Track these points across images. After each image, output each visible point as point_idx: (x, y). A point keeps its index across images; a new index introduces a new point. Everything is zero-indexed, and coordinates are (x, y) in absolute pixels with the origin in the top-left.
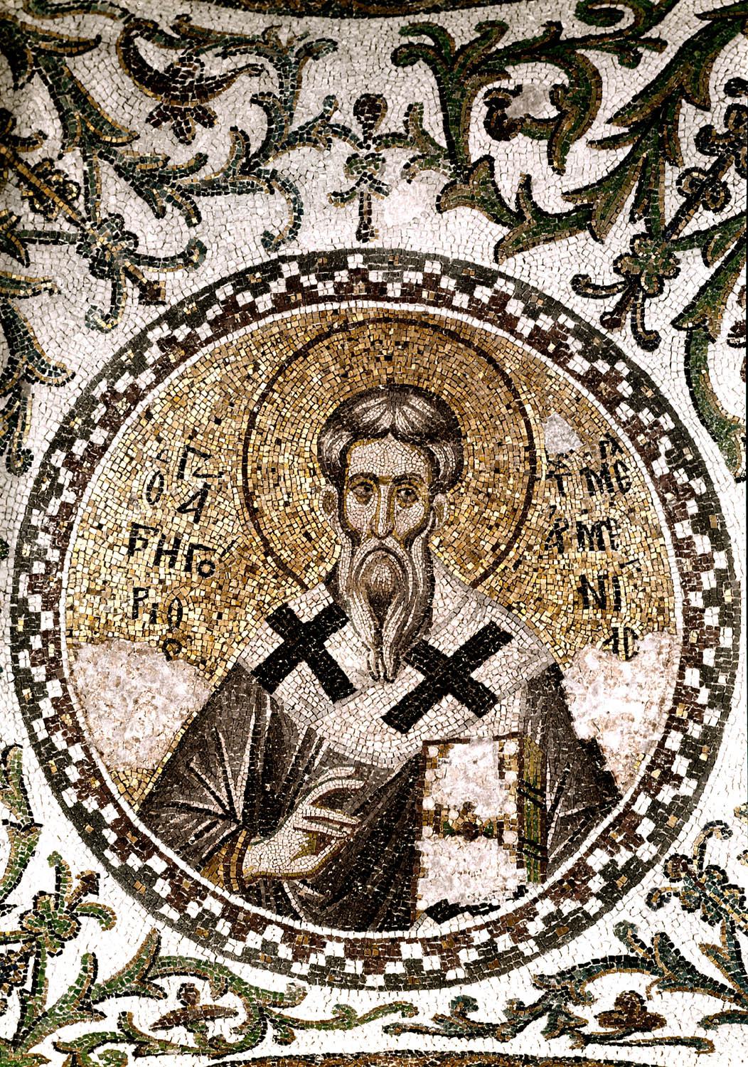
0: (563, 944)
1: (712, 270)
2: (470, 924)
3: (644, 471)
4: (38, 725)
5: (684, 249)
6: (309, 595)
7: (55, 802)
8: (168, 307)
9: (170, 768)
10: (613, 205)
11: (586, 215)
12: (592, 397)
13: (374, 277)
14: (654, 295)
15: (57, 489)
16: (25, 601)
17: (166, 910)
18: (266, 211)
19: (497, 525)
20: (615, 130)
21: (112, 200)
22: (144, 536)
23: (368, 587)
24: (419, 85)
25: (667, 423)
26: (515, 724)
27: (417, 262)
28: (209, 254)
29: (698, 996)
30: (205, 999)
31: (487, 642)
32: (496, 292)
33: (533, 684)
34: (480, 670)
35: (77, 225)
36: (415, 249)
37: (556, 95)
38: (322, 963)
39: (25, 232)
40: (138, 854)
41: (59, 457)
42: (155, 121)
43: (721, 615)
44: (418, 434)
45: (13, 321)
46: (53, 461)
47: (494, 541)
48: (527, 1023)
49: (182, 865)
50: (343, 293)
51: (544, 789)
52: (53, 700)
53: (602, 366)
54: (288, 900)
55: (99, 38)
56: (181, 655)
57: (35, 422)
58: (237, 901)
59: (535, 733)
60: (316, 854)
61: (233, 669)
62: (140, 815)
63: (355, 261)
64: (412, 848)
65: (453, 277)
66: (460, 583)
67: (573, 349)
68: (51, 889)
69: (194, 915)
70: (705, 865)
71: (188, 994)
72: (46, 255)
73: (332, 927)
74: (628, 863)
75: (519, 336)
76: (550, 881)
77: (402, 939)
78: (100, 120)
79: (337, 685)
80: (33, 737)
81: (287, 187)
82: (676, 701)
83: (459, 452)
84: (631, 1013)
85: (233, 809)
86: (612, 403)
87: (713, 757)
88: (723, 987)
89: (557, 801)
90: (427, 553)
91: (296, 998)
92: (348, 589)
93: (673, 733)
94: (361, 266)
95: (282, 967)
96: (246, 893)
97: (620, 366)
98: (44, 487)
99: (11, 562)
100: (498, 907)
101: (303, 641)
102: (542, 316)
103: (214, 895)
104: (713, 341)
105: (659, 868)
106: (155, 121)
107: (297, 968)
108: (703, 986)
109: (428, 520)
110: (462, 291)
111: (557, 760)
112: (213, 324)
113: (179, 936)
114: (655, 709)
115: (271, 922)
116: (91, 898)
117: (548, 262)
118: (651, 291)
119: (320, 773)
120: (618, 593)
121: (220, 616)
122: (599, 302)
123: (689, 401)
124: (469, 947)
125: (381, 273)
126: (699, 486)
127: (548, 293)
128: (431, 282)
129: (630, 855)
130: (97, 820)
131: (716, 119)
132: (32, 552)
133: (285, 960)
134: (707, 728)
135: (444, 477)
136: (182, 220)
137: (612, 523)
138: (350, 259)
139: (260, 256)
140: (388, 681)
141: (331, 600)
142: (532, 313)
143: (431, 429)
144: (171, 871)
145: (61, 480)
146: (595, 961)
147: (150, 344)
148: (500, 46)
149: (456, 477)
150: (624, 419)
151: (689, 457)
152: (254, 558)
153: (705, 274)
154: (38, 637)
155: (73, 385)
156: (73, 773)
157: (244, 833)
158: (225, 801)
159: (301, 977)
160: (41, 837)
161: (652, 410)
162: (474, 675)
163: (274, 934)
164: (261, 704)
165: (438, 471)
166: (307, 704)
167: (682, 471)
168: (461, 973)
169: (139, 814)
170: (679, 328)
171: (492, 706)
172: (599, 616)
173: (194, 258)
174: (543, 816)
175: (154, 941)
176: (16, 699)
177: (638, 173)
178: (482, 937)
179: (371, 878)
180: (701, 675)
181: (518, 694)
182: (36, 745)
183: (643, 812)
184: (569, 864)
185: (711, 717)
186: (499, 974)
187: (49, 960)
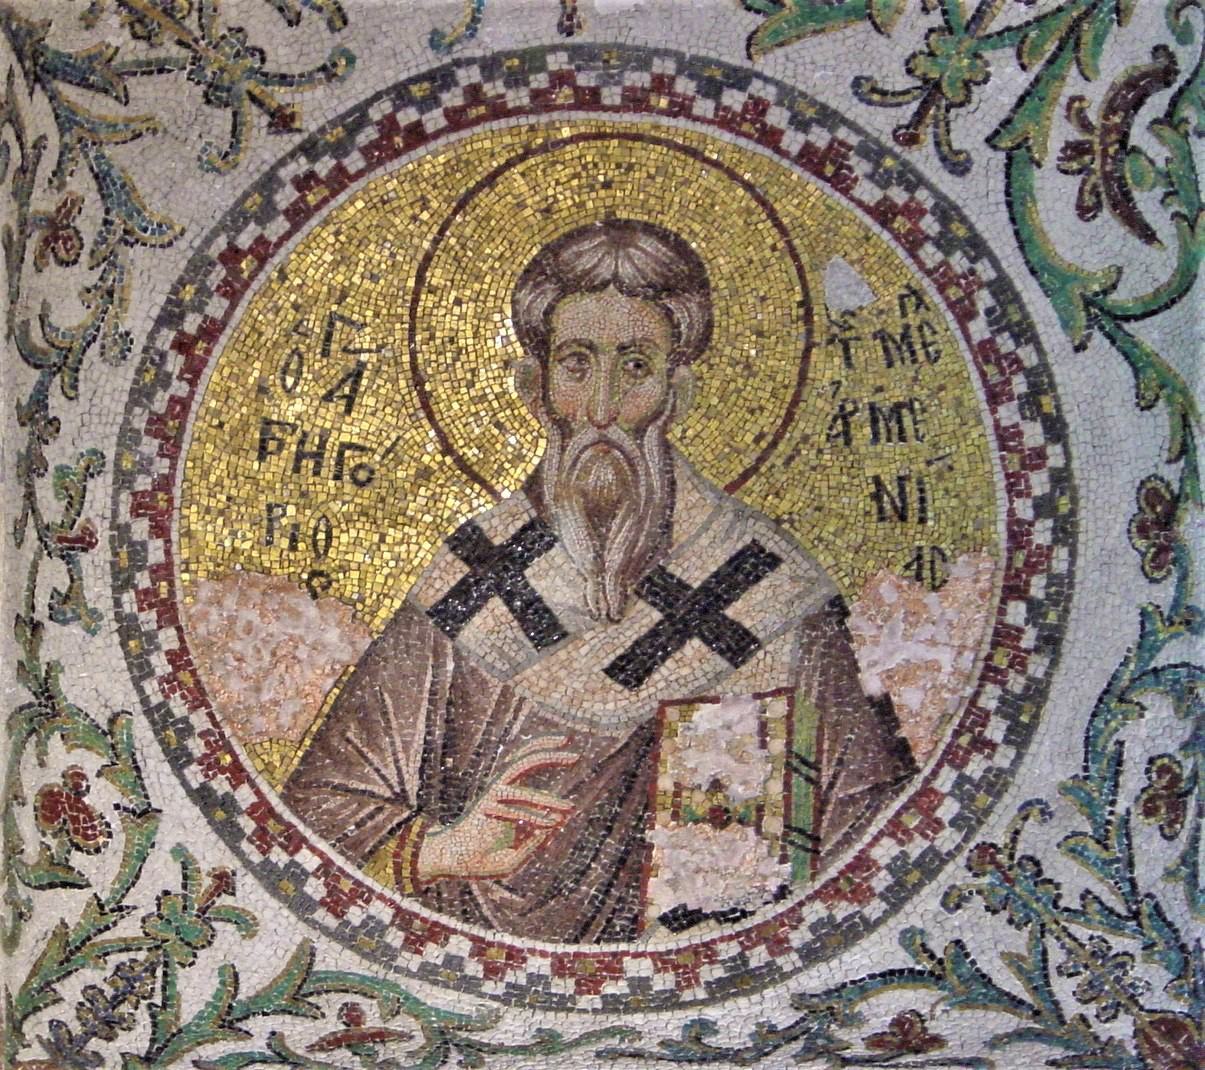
0: (834, 956)
1: (1032, 77)
2: (716, 935)
3: (958, 334)
4: (151, 687)
5: (994, 48)
6: (504, 508)
7: (175, 781)
8: (306, 135)
9: (320, 739)
12: (886, 236)
13: (584, 80)
14: (961, 105)
15: (164, 381)
16: (128, 526)
17: (321, 915)
19: (762, 409)
22: (279, 435)
23: (584, 494)
26: (783, 677)
27: (642, 58)
28: (359, 63)
29: (992, 1015)
30: (372, 1020)
31: (749, 566)
32: (751, 97)
33: (811, 623)
34: (738, 604)
35: (188, 46)
36: (638, 42)
38: (523, 981)
39: (123, 64)
40: (284, 848)
41: (167, 336)
43: (1054, 530)
44: (650, 285)
45: (108, 174)
46: (158, 344)
47: (756, 430)
48: (776, 1047)
49: (339, 861)
50: (541, 101)
51: (819, 761)
52: (167, 653)
53: (898, 195)
54: (477, 905)
56: (331, 591)
57: (134, 295)
58: (411, 905)
59: (809, 686)
60: (515, 847)
61: (402, 609)
62: (286, 798)
63: (557, 62)
64: (643, 840)
65: (691, 77)
66: (713, 488)
69: (356, 922)
70: (1018, 855)
71: (352, 1015)
72: (150, 88)
73: (536, 938)
74: (923, 855)
75: (785, 154)
76: (823, 878)
77: (626, 953)
79: (541, 624)
80: (145, 701)
82: (995, 645)
83: (707, 307)
84: (906, 1034)
85: (403, 791)
86: (913, 243)
87: (1036, 717)
88: (1021, 1002)
89: (835, 776)
90: (666, 447)
91: (490, 1021)
92: (556, 498)
93: (989, 687)
94: (565, 67)
95: (469, 985)
96: (422, 893)
97: (922, 195)
98: (148, 378)
99: (110, 478)
100: (753, 913)
102: (815, 129)
103: (381, 897)
104: (1039, 165)
105: (961, 860)
107: (489, 987)
108: (998, 1001)
109: (665, 402)
110: (706, 95)
111: (837, 723)
112: (366, 151)
113: (338, 947)
114: (969, 655)
115: (454, 931)
116: (225, 900)
117: (819, 59)
118: (958, 100)
119: (516, 743)
120: (922, 500)
121: (382, 539)
122: (892, 111)
123: (1014, 243)
124: (712, 962)
125: (593, 74)
126: (1028, 356)
127: (821, 99)
128: (661, 84)
129: (926, 844)
130: (228, 803)
132: (134, 463)
133: (474, 978)
134: (1031, 679)
135: (688, 344)
136: (323, 25)
137: (917, 405)
138: (550, 58)
139: (430, 61)
140: (612, 621)
141: (534, 514)
142: (801, 124)
143: (667, 279)
145: (169, 367)
146: (872, 977)
147: (282, 184)
149: (704, 342)
150: (930, 265)
151: (1016, 318)
152: (426, 459)
153: (1023, 80)
154: (146, 573)
155: (182, 244)
156: (197, 747)
157: (418, 822)
158: (394, 781)
159: (494, 998)
160: (161, 825)
161: (965, 253)
162: (729, 612)
163: (459, 946)
164: (438, 653)
165: (679, 336)
166: (502, 654)
167: (1006, 335)
168: (702, 994)
169: (282, 796)
170: (995, 148)
171: (752, 653)
172: (898, 531)
173: (340, 71)
174: (817, 795)
175: (307, 953)
176: (121, 654)
179: (591, 881)
180: (1029, 610)
181: (790, 637)
182: (148, 712)
183: (946, 789)
184: (848, 856)
185: (1037, 666)
186: (746, 993)
187: (180, 971)
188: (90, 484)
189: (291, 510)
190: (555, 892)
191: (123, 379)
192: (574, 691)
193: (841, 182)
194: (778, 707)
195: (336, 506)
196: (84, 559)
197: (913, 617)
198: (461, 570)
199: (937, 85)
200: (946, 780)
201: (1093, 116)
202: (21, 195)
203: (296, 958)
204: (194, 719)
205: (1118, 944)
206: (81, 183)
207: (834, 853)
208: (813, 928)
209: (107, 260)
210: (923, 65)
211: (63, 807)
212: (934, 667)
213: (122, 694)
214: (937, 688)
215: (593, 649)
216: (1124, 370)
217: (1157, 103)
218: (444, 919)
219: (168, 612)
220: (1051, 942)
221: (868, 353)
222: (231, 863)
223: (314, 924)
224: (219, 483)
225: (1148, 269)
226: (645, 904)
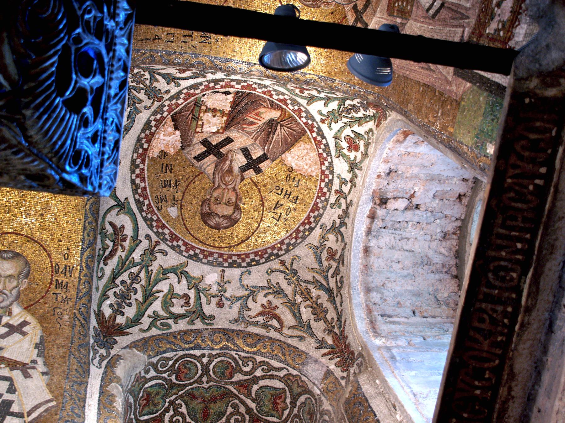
4: (329, 160)
9: (296, 141)
10: (158, 274)
11: (165, 272)
12: (164, 222)
13: (221, 260)
15: (314, 217)
17: (304, 110)
18: (250, 281)
20: (157, 295)
21: (289, 289)
24: (208, 310)
25: (144, 214)
27: (209, 263)
31: (199, 158)
33: (189, 146)
37: (173, 305)
41: (313, 225)
49: (297, 118)
50: (230, 256)
53: (160, 230)
55: (289, 329)
57: (318, 236)
63: (226, 264)
67: (168, 235)
68: (333, 123)
71: (302, 92)
75: (182, 240)
76: (195, 97)
78: (290, 309)
79: (246, 152)
80: (331, 158)
81: (243, 286)
83: (202, 210)
86: (158, 220)
90: (214, 182)
92: (238, 176)
95: (275, 90)
96: (282, 109)
97: (155, 230)
101: (253, 164)
105: (165, 99)
107: (271, 89)
112: (266, 253)
114: (157, 137)
116: (323, 118)
119: (255, 131)
126: (137, 197)
128: (205, 257)
131: (133, 297)
134: (144, 133)
139: (252, 269)
142: (179, 246)
144: (300, 117)
148: (188, 318)
149: (203, 202)
150: (155, 216)
153: (133, 255)
155: (306, 243)
156: (322, 146)
158: (282, 129)
162: (206, 149)
163: (275, 97)
164: (268, 150)
166: (255, 148)
177: (151, 283)
181: (194, 143)
188: (334, 202)
189: (294, 185)
190: (253, 102)
191: (323, 220)
192: (240, 139)
193: (171, 233)
194: (198, 130)
195: (284, 184)
196: (338, 188)
197: (167, 145)
198: (261, 165)
199: (151, 254)
200: (165, 114)
201: (120, 247)
202: (337, 269)
203: (311, 104)
204: (322, 152)
205: (134, 84)
206: (325, 263)
207: (191, 102)
208: (199, 88)
210: (153, 258)
211: (353, 147)
212: (164, 135)
214: (164, 131)
215: (236, 145)
217: (107, 253)
218: (278, 102)
219: (323, 172)
220: (148, 84)
221: (169, 198)
222: (320, 124)
223: (306, 108)
224: (307, 194)
225: (111, 217)
226: (234, 97)
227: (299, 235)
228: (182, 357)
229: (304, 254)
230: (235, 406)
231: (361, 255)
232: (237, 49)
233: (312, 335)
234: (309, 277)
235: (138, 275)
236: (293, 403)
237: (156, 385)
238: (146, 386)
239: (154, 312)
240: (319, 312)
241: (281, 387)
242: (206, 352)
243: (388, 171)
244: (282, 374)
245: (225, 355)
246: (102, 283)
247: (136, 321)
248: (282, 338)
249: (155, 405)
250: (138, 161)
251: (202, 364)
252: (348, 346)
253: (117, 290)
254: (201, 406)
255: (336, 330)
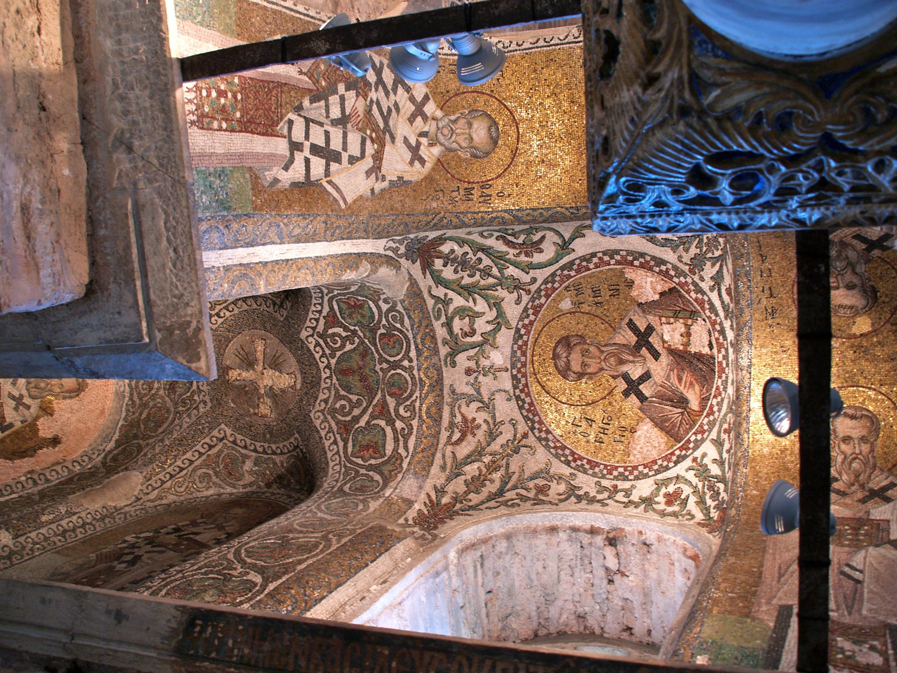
4: (651, 474)
10: (494, 297)
11: (496, 305)
13: (519, 365)
17: (705, 436)
18: (499, 399)
20: (471, 300)
24: (461, 358)
25: (559, 272)
27: (514, 353)
31: (632, 325)
33: (644, 312)
41: (573, 464)
42: (474, 435)
50: (524, 375)
53: (543, 293)
71: (725, 431)
79: (646, 377)
81: (493, 394)
83: (573, 336)
90: (606, 345)
95: (722, 400)
96: (702, 411)
97: (542, 288)
106: (474, 435)
107: (723, 395)
128: (520, 348)
131: (465, 274)
139: (514, 401)
144: (695, 433)
153: (511, 267)
156: (665, 463)
163: (715, 402)
164: (652, 402)
178: (717, 334)
184: (695, 304)
191: (580, 475)
192: (660, 368)
193: (541, 306)
196: (619, 488)
197: (641, 287)
198: (633, 396)
200: (676, 280)
202: (528, 499)
205: (705, 241)
206: (531, 484)
209: (551, 478)
210: (511, 290)
211: (671, 499)
213: (651, 481)
215: (652, 365)
216: (577, 240)
217: (510, 238)
219: (635, 468)
220: (708, 256)
221: (581, 298)
222: (691, 457)
225: (551, 237)
227: (559, 450)
228: (406, 337)
229: (538, 458)
230: (359, 403)
231: (548, 524)
232: (764, 351)
233: (449, 480)
234: (513, 468)
235: (489, 275)
236: (370, 468)
237: (372, 313)
238: (370, 302)
239: (451, 299)
240: (475, 484)
241: (387, 452)
242: (415, 363)
243: (648, 542)
244: (401, 450)
245: (414, 384)
246: (476, 238)
247: (439, 281)
248: (440, 446)
249: (350, 316)
250: (618, 257)
251: (401, 360)
252: (442, 521)
253: (470, 255)
254: (356, 367)
255: (458, 506)
